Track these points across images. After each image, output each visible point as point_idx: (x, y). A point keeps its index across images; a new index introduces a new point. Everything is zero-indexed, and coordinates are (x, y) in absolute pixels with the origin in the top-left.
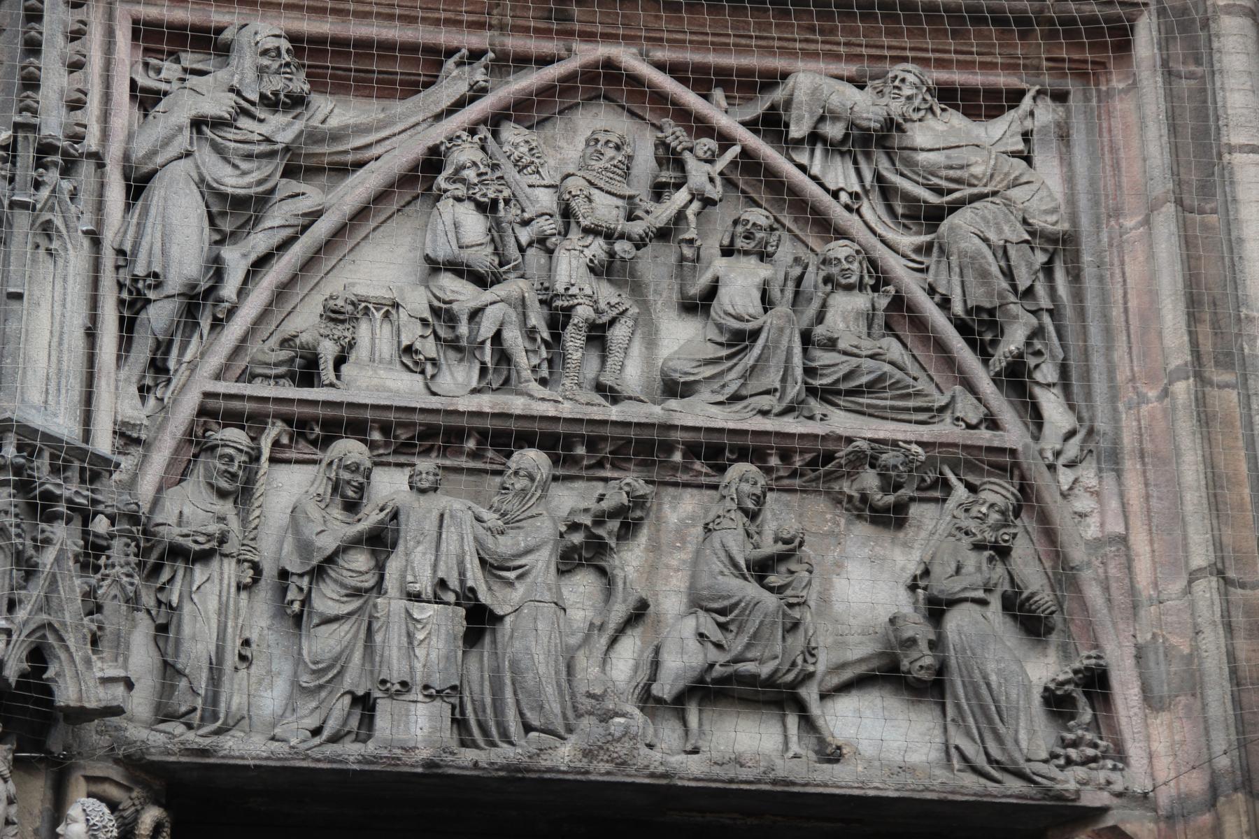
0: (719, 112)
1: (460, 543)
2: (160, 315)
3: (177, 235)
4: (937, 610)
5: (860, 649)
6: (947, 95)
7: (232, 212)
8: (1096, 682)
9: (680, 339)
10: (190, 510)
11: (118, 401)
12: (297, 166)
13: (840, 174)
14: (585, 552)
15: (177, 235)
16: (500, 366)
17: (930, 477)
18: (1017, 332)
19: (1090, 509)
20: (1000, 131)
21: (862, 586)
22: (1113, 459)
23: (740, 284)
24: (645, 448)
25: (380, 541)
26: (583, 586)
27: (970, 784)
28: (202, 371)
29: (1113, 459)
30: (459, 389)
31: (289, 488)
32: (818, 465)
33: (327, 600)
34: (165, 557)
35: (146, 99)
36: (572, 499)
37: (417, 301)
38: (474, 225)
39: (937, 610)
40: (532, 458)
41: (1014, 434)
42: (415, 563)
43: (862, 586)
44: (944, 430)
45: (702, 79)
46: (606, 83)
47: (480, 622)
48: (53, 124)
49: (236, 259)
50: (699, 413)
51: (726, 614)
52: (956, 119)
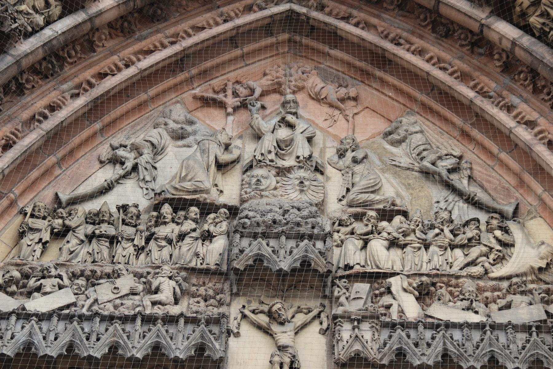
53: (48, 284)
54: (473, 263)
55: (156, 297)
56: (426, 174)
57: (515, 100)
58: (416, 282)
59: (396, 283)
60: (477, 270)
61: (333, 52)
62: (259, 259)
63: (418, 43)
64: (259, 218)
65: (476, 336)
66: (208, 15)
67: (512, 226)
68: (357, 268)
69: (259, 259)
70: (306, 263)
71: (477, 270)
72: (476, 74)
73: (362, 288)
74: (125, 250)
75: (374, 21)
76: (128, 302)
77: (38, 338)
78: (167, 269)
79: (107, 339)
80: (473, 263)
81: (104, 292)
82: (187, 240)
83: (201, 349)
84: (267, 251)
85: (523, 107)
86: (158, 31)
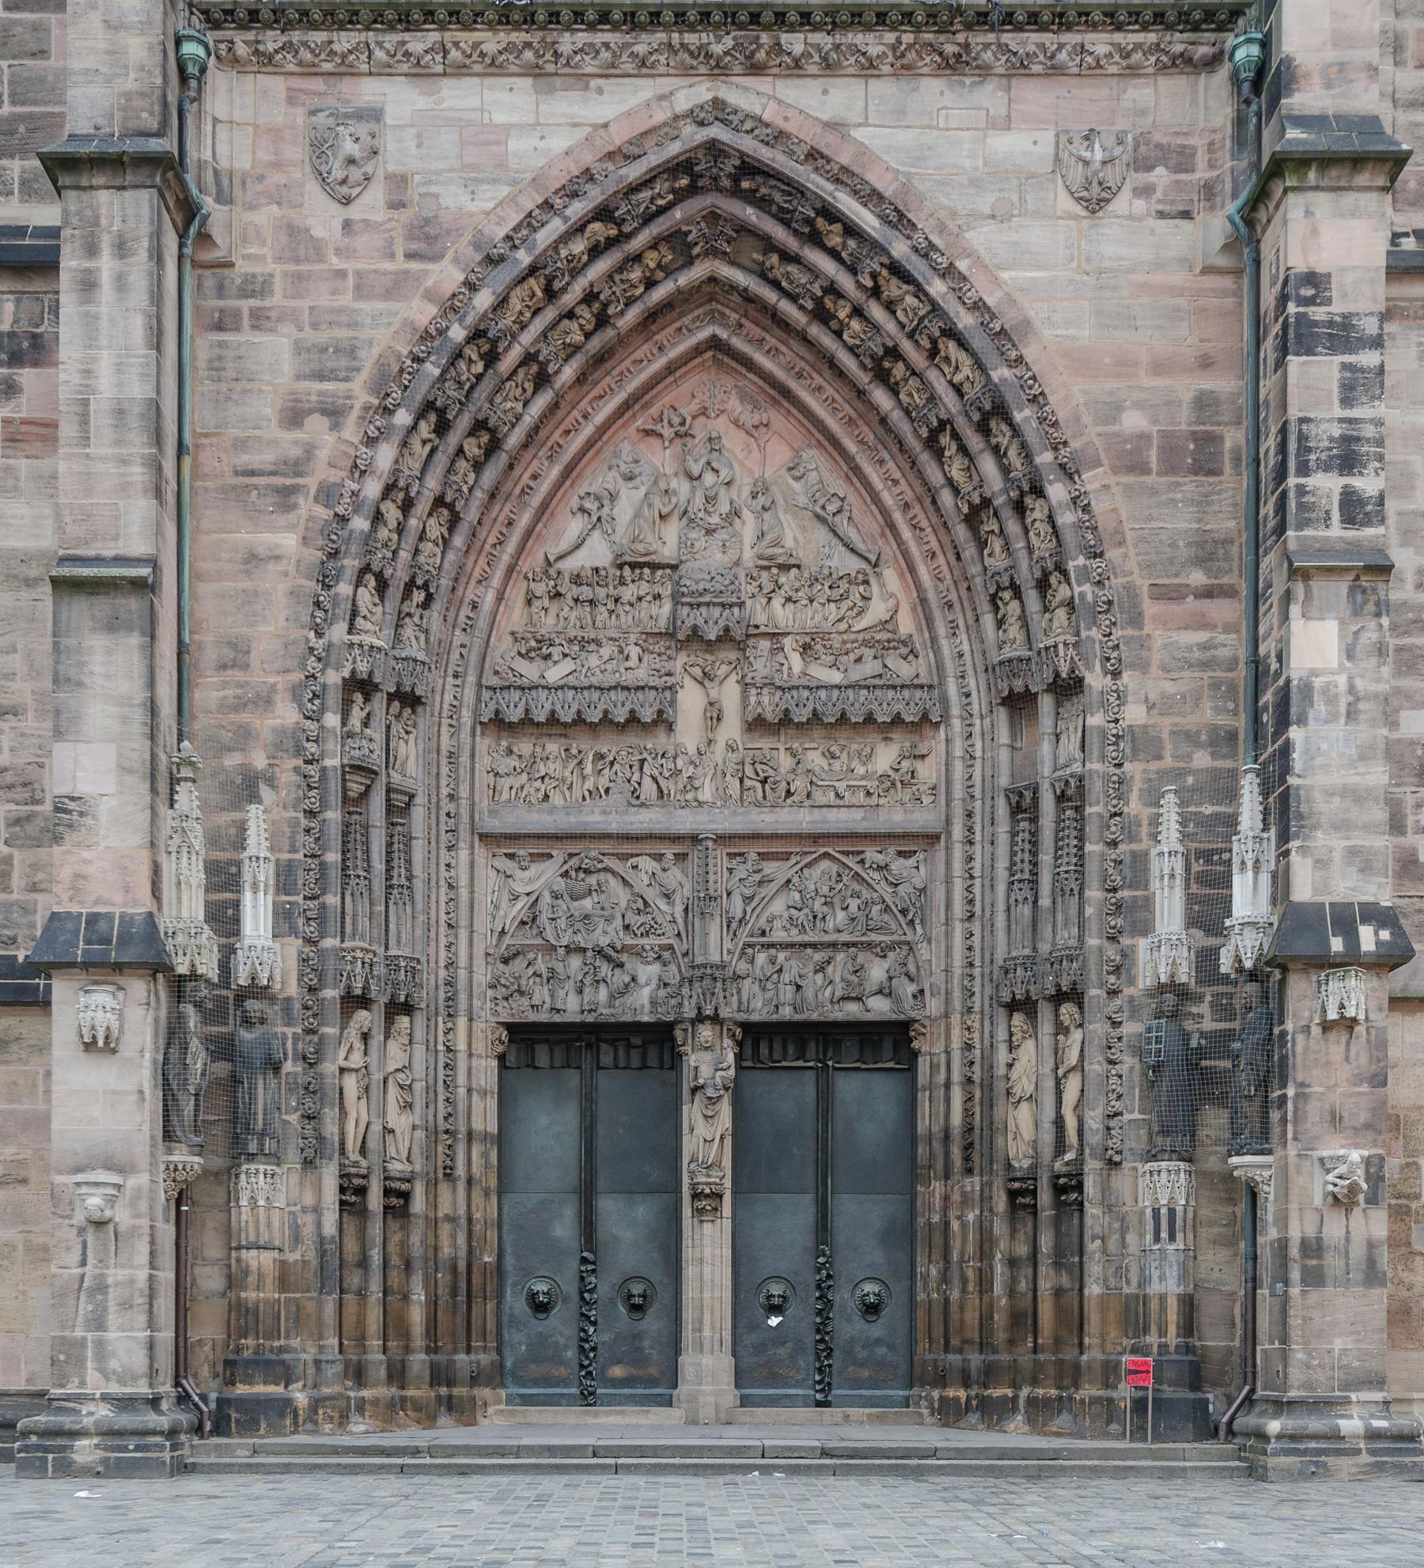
0: (850, 862)
1: (794, 971)
2: (734, 925)
3: (737, 907)
4: (890, 978)
5: (875, 988)
6: (900, 853)
7: (748, 900)
8: (922, 991)
9: (841, 916)
10: (742, 967)
11: (728, 945)
12: (761, 883)
13: (876, 876)
14: (820, 969)
15: (737, 907)
16: (803, 930)
17: (892, 947)
18: (912, 912)
19: (924, 952)
20: (912, 862)
21: (877, 971)
22: (929, 942)
23: (854, 904)
24: (833, 945)
25: (780, 971)
26: (820, 975)
27: (894, 1017)
28: (743, 938)
29: (929, 942)
30: (795, 936)
31: (761, 958)
32: (869, 946)
33: (769, 986)
34: (737, 978)
35: (730, 870)
36: (818, 956)
37: (786, 915)
38: (797, 896)
39: (890, 978)
40: (809, 951)
41: (909, 938)
42: (786, 977)
43: (877, 971)
44: (895, 937)
45: (847, 853)
46: (826, 855)
47: (799, 987)
48: (711, 892)
49: (749, 910)
50: (845, 937)
51: (848, 983)
52: (902, 860)
53: (556, 651)
54: (840, 620)
55: (628, 664)
56: (818, 517)
57: (887, 457)
58: (802, 640)
59: (788, 642)
60: (843, 626)
61: (750, 376)
62: (695, 629)
63: (818, 380)
64: (694, 588)
65: (836, 693)
66: (645, 347)
67: (873, 581)
68: (763, 629)
69: (695, 629)
70: (727, 629)
71: (843, 626)
72: (860, 422)
73: (765, 645)
74: (602, 613)
75: (783, 348)
76: (609, 667)
77: (558, 708)
78: (633, 638)
79: (601, 707)
80: (840, 620)
81: (593, 661)
82: (644, 604)
83: (660, 712)
84: (700, 622)
85: (891, 464)
86: (608, 373)
